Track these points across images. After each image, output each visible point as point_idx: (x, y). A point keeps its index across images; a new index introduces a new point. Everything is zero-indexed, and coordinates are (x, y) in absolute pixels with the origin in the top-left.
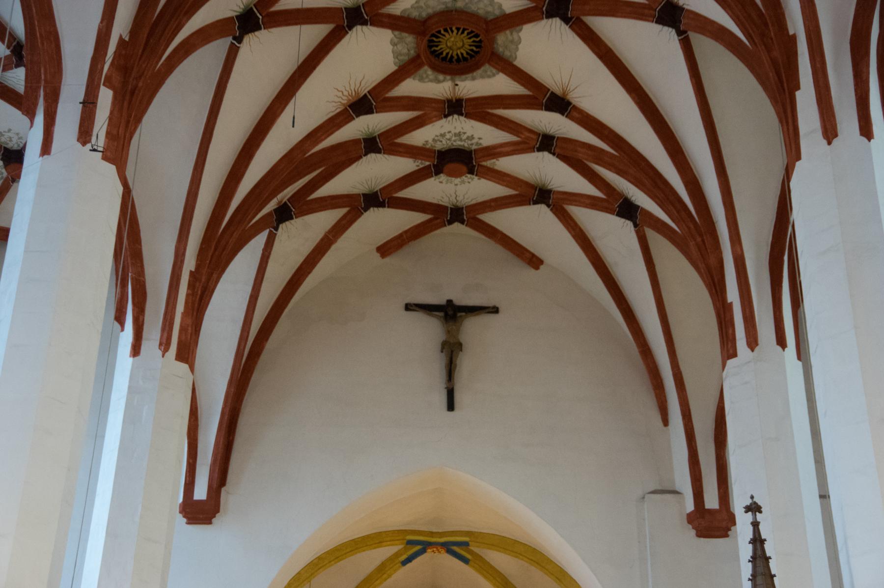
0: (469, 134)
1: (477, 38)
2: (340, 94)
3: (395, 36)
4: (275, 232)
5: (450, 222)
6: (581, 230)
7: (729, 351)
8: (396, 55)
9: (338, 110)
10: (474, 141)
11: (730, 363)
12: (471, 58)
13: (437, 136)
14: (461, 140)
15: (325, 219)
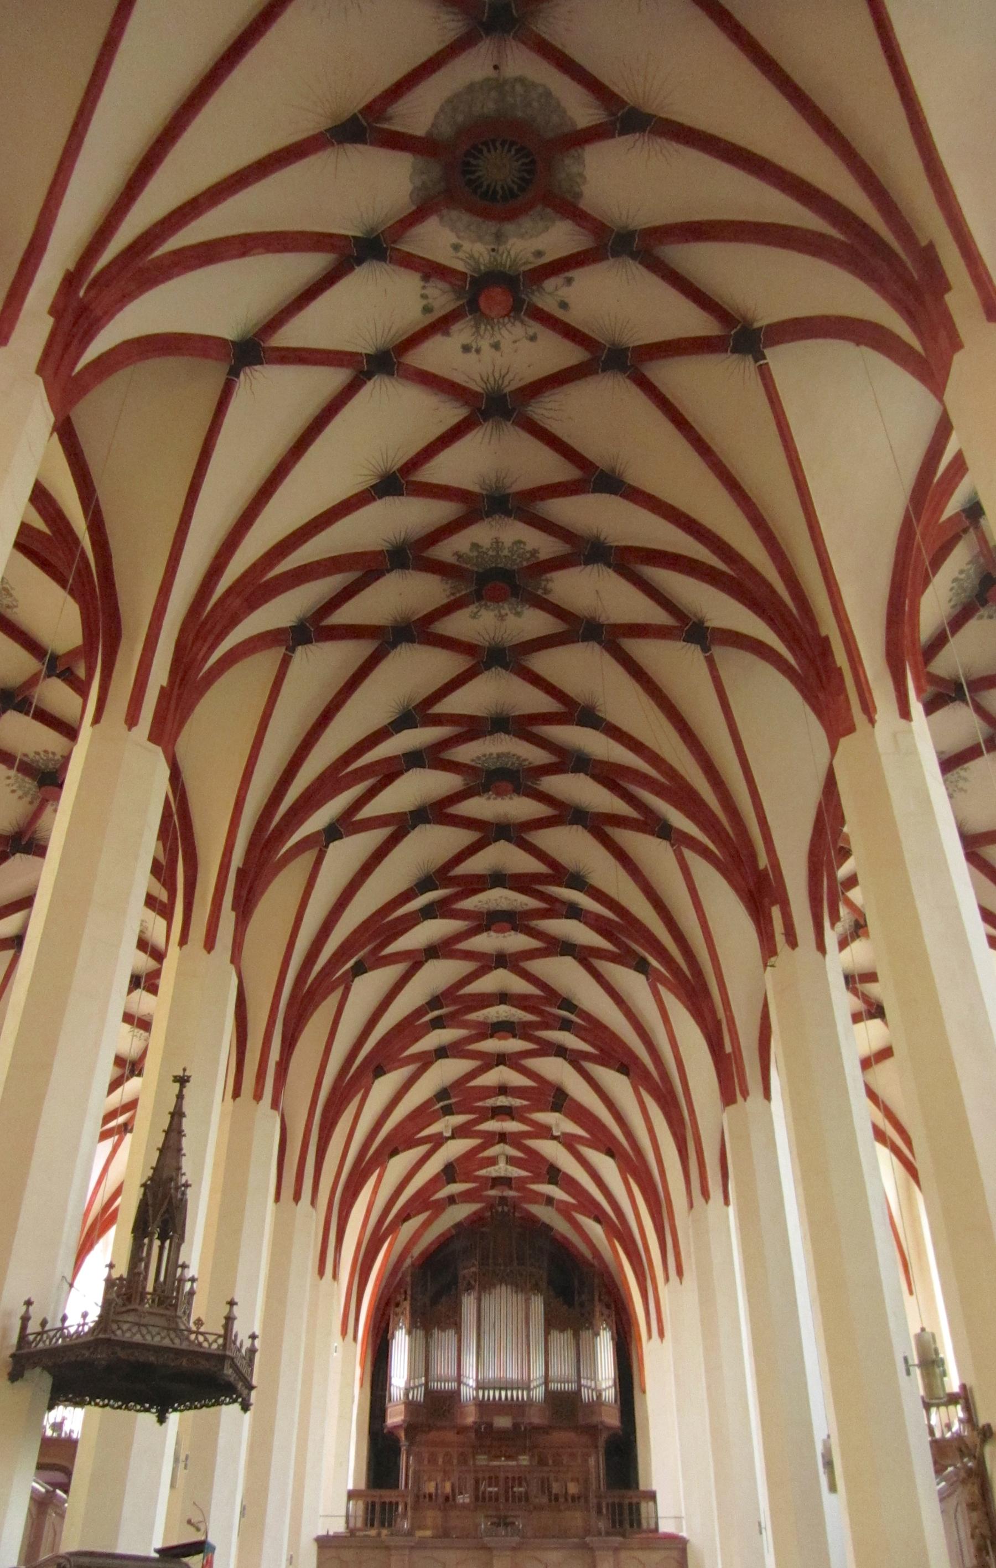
8: (580, 160)
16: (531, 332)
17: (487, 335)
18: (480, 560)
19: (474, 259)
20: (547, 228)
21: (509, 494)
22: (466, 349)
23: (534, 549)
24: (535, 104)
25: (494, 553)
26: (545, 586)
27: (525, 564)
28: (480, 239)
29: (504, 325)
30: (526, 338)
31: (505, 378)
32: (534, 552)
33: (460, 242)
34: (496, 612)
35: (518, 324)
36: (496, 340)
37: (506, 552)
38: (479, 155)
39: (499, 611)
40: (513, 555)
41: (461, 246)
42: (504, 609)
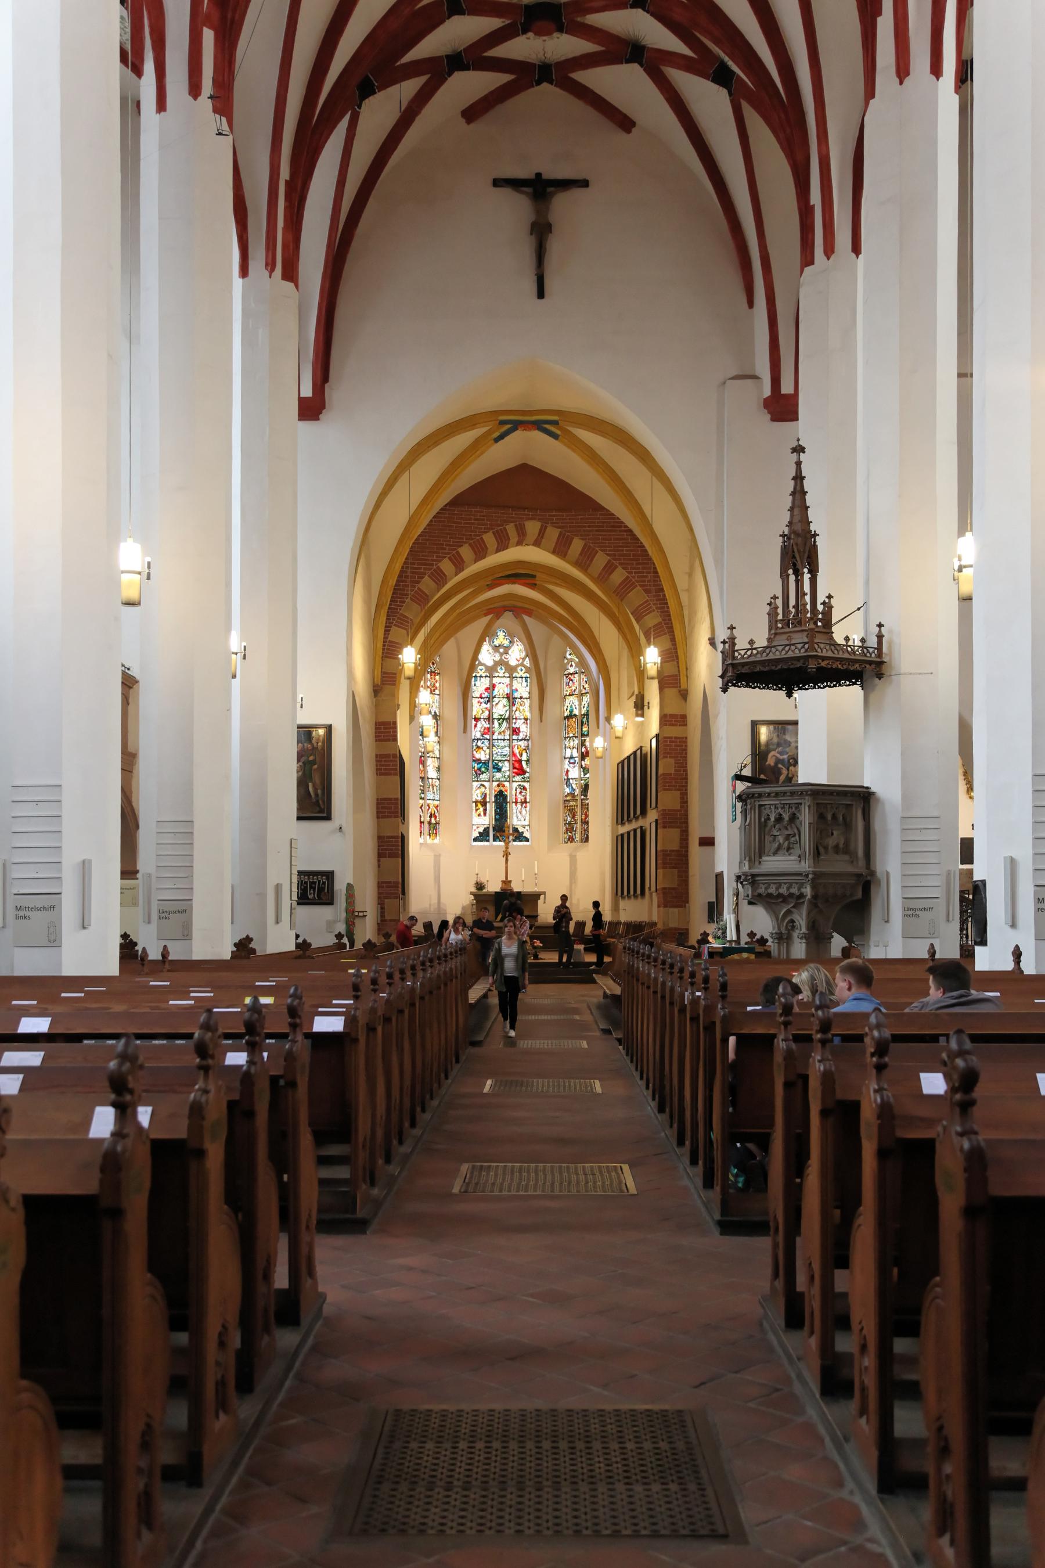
4: (358, 110)
5: (539, 83)
6: (676, 92)
7: (808, 260)
11: (807, 270)
15: (410, 87)
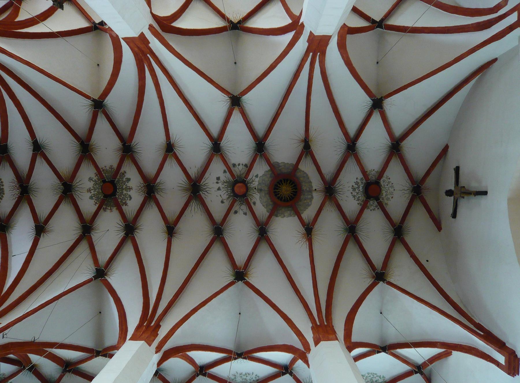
0: (354, 184)
1: (288, 181)
2: (300, 242)
3: (280, 216)
8: (290, 215)
9: (308, 243)
10: (359, 181)
12: (294, 183)
13: (355, 199)
14: (359, 187)
16: (224, 201)
17: (223, 186)
18: (121, 182)
19: (253, 182)
20: (263, 206)
21: (154, 193)
22: (218, 179)
23: (127, 204)
24: (305, 201)
25: (124, 188)
26: (108, 209)
27: (119, 200)
28: (259, 184)
29: (227, 192)
30: (222, 200)
31: (206, 192)
32: (126, 204)
33: (259, 177)
34: (92, 188)
35: (228, 196)
36: (221, 189)
37: (125, 192)
38: (290, 184)
39: (92, 190)
40: (123, 195)
41: (257, 178)
42: (94, 192)
